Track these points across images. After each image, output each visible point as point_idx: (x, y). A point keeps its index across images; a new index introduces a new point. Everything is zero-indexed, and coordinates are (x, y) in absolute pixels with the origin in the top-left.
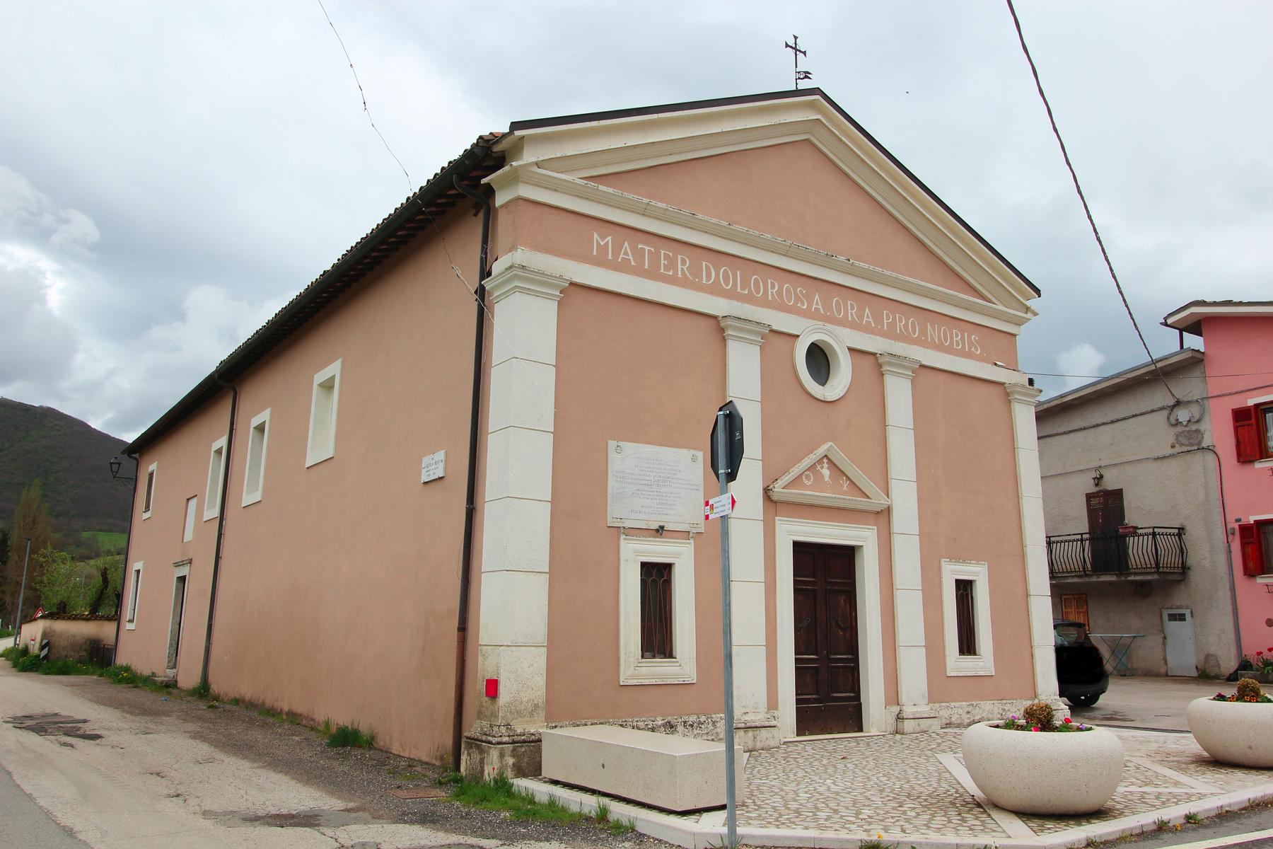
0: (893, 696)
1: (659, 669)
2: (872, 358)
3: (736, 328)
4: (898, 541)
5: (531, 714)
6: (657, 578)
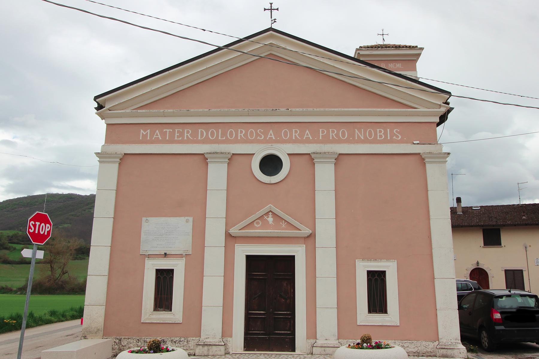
1: (163, 316)
2: (307, 156)
4: (319, 253)
5: (96, 333)
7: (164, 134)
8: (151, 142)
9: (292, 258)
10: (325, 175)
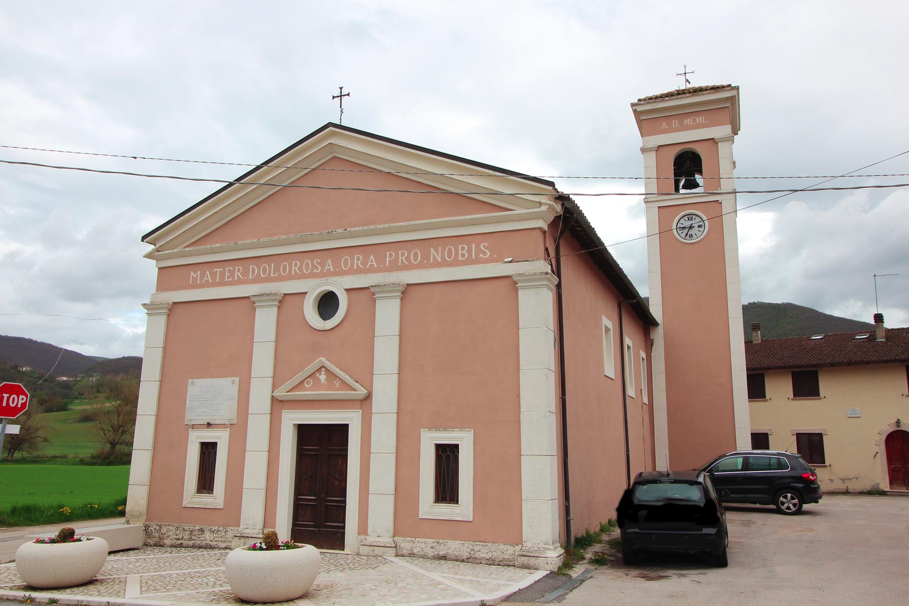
0: (363, 529)
3: (259, 301)
4: (375, 419)
6: (208, 451)
7: (213, 275)
8: (202, 286)
10: (388, 314)
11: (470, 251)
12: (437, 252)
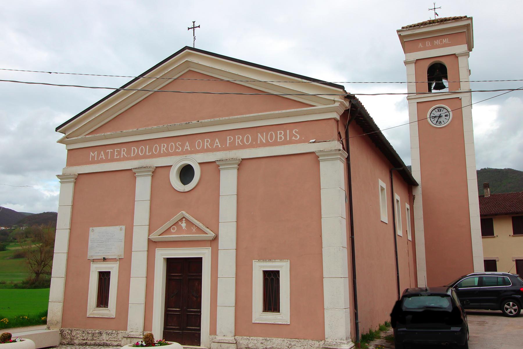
0: (213, 331)
3: (138, 172)
4: (221, 254)
5: (56, 325)
6: (104, 278)
7: (106, 154)
9: (200, 259)
10: (229, 180)
11: (285, 135)
12: (263, 137)
